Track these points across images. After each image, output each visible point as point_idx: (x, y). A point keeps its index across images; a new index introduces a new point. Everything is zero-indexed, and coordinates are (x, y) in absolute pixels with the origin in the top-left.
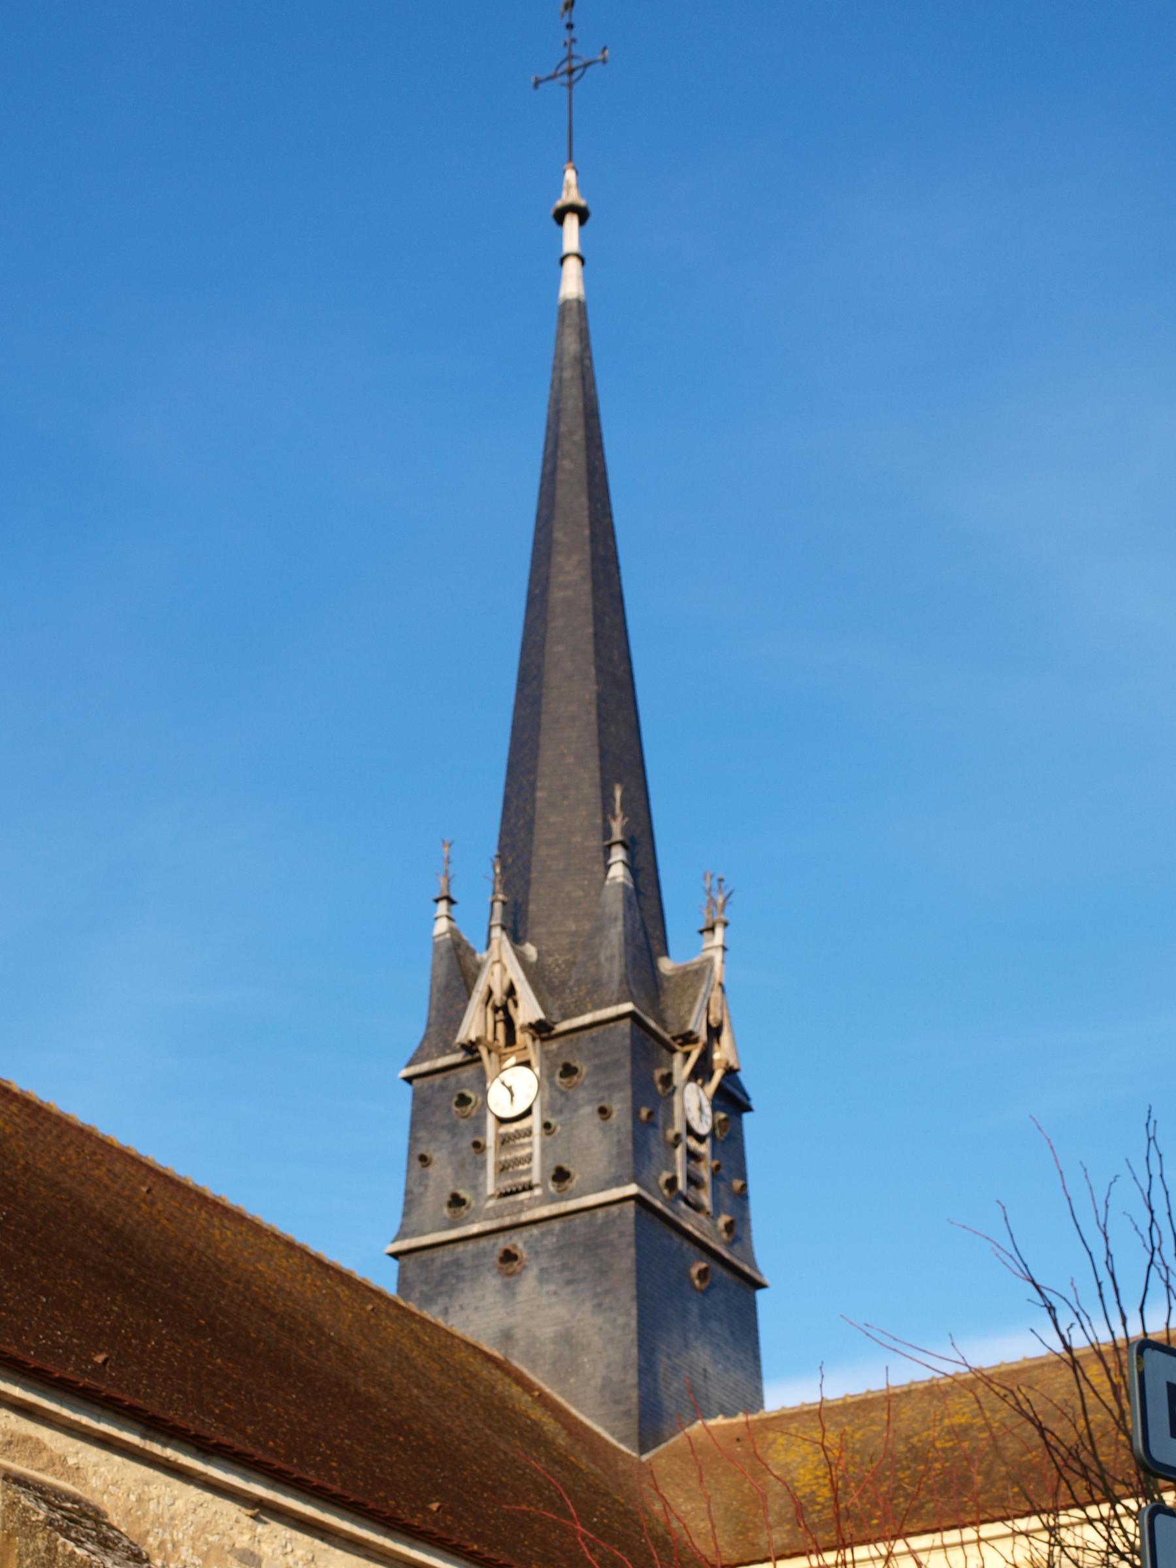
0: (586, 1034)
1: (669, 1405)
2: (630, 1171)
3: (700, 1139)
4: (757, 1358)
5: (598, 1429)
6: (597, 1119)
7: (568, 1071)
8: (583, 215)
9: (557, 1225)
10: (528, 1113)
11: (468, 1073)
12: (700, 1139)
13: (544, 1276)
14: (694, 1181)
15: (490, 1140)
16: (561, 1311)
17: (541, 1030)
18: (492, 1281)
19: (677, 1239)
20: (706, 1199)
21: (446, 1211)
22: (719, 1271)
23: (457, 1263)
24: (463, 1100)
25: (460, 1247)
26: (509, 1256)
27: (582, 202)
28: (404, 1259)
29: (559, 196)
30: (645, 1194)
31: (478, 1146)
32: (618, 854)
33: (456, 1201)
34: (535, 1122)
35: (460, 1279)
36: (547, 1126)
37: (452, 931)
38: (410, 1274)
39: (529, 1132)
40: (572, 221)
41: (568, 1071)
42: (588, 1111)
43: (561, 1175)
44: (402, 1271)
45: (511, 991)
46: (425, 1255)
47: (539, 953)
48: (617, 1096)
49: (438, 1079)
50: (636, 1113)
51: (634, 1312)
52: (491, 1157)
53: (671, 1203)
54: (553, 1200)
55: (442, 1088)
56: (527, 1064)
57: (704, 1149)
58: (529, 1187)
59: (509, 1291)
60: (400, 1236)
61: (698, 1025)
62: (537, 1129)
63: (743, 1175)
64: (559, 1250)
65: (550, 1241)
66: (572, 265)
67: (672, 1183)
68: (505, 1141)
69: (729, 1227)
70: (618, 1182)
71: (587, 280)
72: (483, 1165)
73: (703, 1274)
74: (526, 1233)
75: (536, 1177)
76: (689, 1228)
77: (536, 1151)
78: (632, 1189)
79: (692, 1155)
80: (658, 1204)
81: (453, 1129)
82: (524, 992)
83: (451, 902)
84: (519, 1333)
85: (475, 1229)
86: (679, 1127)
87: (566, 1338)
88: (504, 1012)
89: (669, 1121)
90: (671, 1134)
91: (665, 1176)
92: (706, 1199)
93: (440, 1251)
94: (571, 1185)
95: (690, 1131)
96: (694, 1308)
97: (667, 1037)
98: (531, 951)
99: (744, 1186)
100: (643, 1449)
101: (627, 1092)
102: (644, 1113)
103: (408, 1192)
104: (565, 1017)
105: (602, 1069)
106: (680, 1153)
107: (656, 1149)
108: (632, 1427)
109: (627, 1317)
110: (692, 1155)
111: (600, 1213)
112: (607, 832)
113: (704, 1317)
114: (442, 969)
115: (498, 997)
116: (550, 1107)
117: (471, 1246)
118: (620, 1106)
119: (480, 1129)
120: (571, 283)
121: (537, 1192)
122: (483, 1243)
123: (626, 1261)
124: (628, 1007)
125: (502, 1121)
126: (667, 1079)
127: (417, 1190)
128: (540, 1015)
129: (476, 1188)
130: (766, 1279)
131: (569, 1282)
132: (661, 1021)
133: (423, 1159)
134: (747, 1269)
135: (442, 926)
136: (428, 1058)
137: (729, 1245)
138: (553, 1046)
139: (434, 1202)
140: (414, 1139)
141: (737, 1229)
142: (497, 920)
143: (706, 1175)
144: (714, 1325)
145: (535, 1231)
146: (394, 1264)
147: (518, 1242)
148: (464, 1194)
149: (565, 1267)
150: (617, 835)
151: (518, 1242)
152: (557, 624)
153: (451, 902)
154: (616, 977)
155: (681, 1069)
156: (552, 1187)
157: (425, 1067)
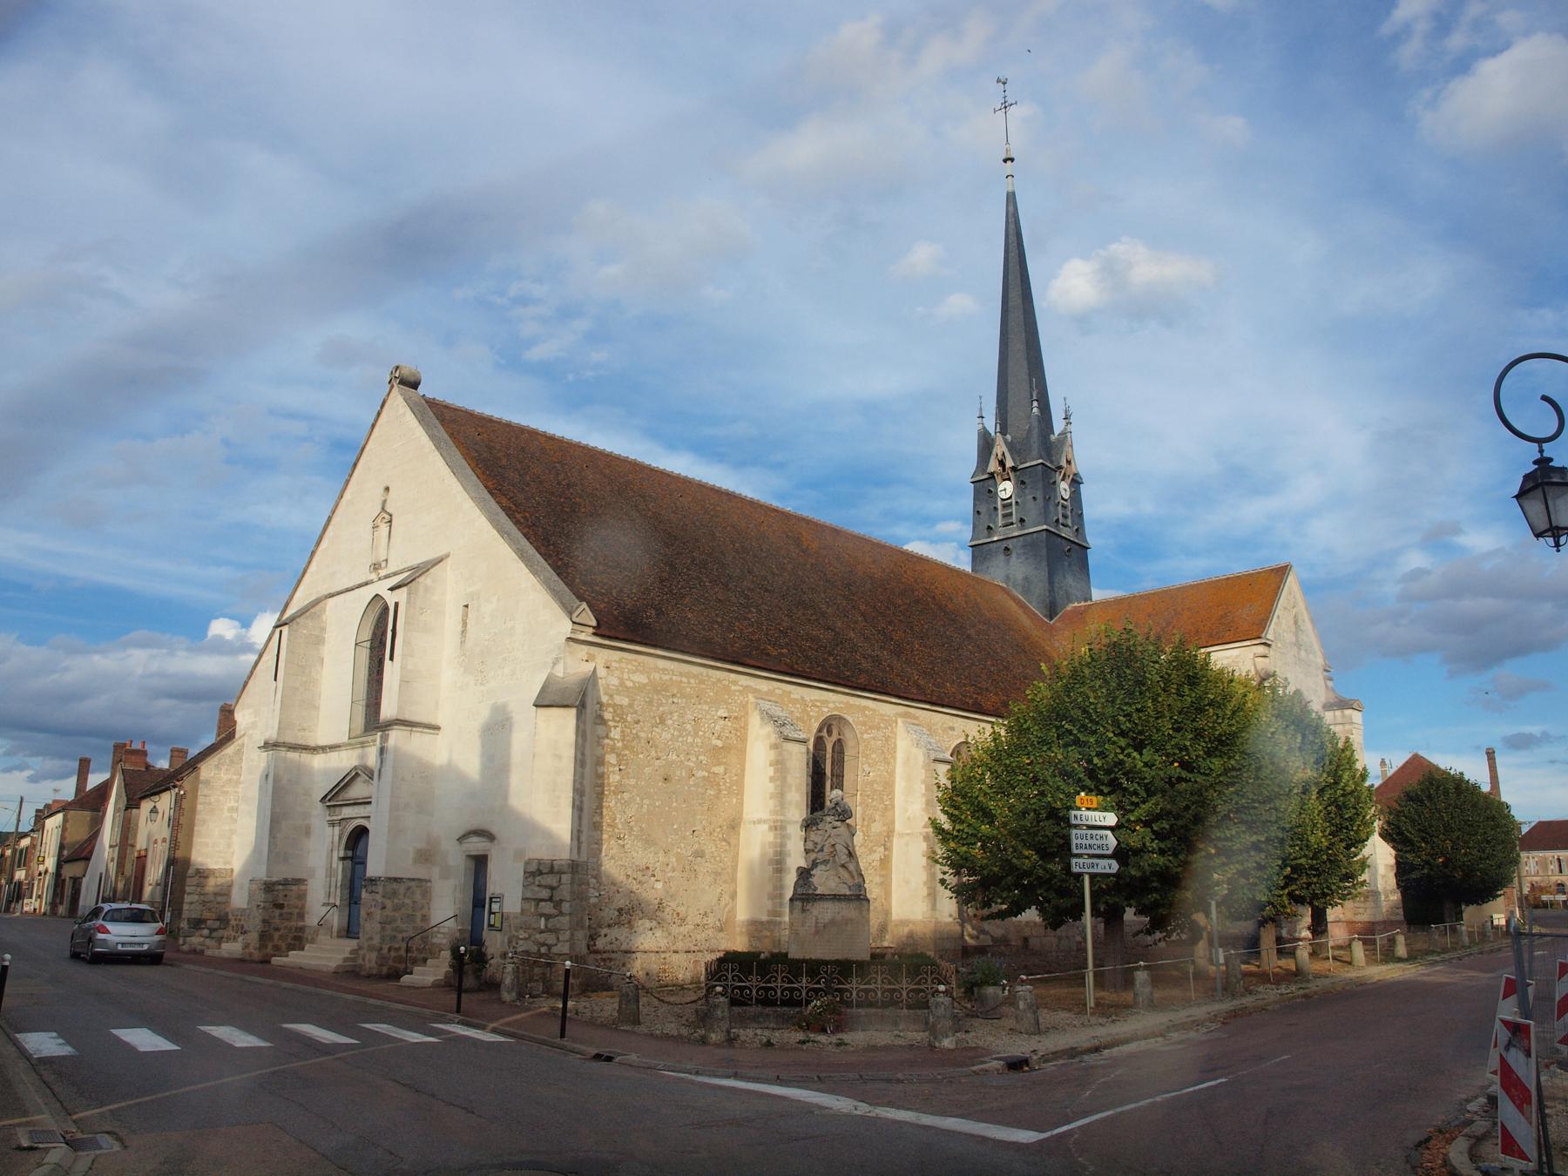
0: (1029, 469)
3: (1066, 500)
6: (1032, 500)
7: (1023, 483)
9: (1021, 539)
10: (1010, 497)
11: (991, 481)
12: (1066, 500)
14: (1065, 516)
15: (999, 506)
17: (1014, 469)
18: (1002, 557)
19: (1059, 539)
21: (986, 531)
23: (990, 550)
24: (990, 491)
25: (991, 545)
26: (1007, 549)
30: (1049, 528)
31: (996, 509)
32: (1035, 404)
33: (989, 528)
36: (1017, 502)
39: (1011, 504)
41: (1023, 483)
42: (1030, 497)
43: (1022, 521)
44: (973, 552)
47: (1012, 437)
48: (1038, 493)
51: (1047, 570)
52: (1000, 513)
53: (1056, 527)
56: (1009, 479)
58: (1012, 524)
59: (1008, 561)
61: (1064, 463)
64: (1024, 546)
67: (1057, 521)
68: (1004, 506)
69: (1077, 530)
72: (997, 515)
74: (1012, 540)
75: (1014, 519)
76: (1063, 535)
79: (1064, 507)
80: (1053, 530)
82: (1008, 455)
84: (1011, 577)
85: (995, 539)
87: (1026, 579)
88: (1002, 463)
89: (1055, 497)
91: (1055, 518)
92: (1069, 522)
93: (985, 546)
94: (1026, 524)
95: (1063, 499)
96: (1066, 563)
97: (1053, 467)
98: (1009, 437)
99: (1082, 513)
100: (1051, 619)
103: (974, 524)
104: (1022, 463)
109: (1044, 574)
111: (1035, 535)
112: (1032, 396)
113: (1070, 565)
114: (981, 443)
115: (1000, 457)
116: (1018, 496)
117: (994, 544)
118: (1039, 495)
119: (996, 502)
121: (1015, 526)
122: (999, 543)
123: (1044, 552)
124: (1040, 461)
125: (1003, 500)
127: (977, 523)
129: (995, 523)
130: (1091, 545)
131: (1027, 559)
132: (1051, 462)
133: (978, 512)
134: (1084, 544)
136: (978, 475)
138: (1018, 473)
139: (983, 528)
140: (975, 505)
141: (1079, 531)
142: (998, 430)
143: (1069, 513)
145: (1015, 540)
146: (971, 549)
147: (1010, 544)
148: (991, 525)
150: (1035, 398)
151: (1010, 544)
153: (983, 417)
157: (977, 479)
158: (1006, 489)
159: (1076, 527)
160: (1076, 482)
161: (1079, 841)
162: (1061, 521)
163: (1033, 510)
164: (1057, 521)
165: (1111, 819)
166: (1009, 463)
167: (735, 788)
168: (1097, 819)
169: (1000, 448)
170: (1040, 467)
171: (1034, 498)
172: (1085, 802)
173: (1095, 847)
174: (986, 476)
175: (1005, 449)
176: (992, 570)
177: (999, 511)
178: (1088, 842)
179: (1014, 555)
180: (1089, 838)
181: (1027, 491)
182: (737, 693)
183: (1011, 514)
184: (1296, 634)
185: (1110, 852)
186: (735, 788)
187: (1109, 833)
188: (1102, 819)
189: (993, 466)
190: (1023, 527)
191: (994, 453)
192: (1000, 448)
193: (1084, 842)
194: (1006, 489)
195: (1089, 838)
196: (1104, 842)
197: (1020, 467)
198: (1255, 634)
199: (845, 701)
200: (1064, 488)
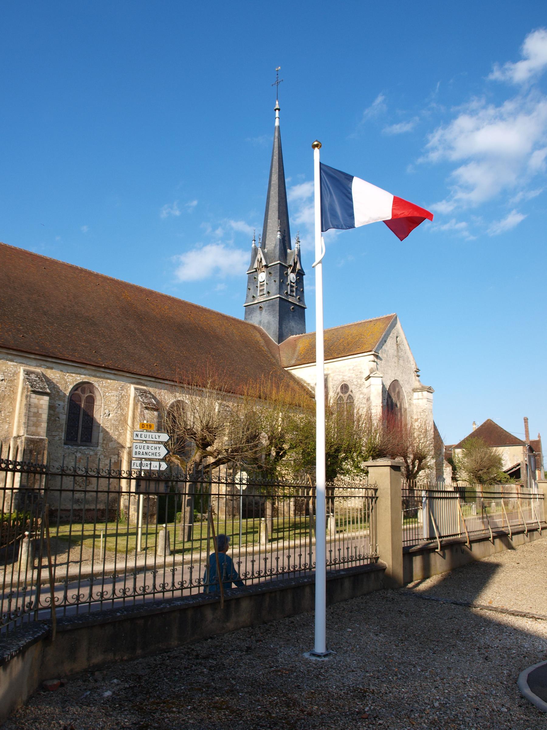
0: (273, 266)
1: (285, 334)
2: (278, 292)
3: (294, 283)
4: (305, 322)
5: (272, 339)
7: (270, 273)
8: (279, 110)
9: (268, 302)
10: (264, 281)
11: (256, 273)
12: (294, 283)
13: (265, 312)
14: (292, 291)
15: (259, 286)
16: (268, 317)
17: (266, 266)
18: (258, 311)
20: (294, 294)
22: (297, 307)
23: (253, 308)
24: (255, 278)
25: (254, 305)
26: (261, 307)
27: (278, 108)
28: (247, 307)
29: (275, 107)
30: (281, 296)
31: (257, 287)
33: (253, 297)
34: (265, 283)
35: (254, 311)
37: (255, 246)
38: (247, 310)
39: (264, 284)
40: (277, 111)
41: (270, 273)
42: (273, 280)
43: (268, 293)
45: (261, 259)
46: (249, 307)
49: (251, 274)
50: (280, 281)
52: (259, 289)
54: (267, 297)
55: (252, 276)
56: (264, 272)
57: (294, 285)
58: (264, 294)
59: (261, 314)
60: (245, 303)
62: (265, 284)
63: (303, 288)
64: (269, 306)
65: (267, 305)
66: (277, 120)
67: (287, 293)
68: (261, 286)
69: (299, 298)
70: (276, 294)
71: (280, 122)
73: (293, 308)
75: (265, 293)
76: (290, 300)
77: (265, 288)
78: (278, 296)
79: (292, 286)
80: (283, 297)
81: (253, 283)
83: (255, 240)
84: (262, 321)
85: (256, 302)
86: (289, 282)
89: (287, 281)
90: (287, 283)
91: (286, 291)
95: (291, 282)
96: (291, 315)
97: (287, 265)
100: (279, 343)
101: (278, 278)
102: (282, 280)
105: (275, 273)
106: (289, 287)
107: (284, 286)
108: (277, 340)
110: (292, 286)
113: (293, 316)
114: (253, 253)
115: (259, 260)
116: (268, 280)
117: (255, 305)
119: (257, 284)
120: (277, 123)
121: (265, 295)
122: (257, 304)
123: (277, 308)
124: (279, 262)
126: (287, 273)
128: (265, 264)
129: (256, 294)
130: (307, 307)
131: (269, 312)
135: (253, 245)
137: (299, 302)
138: (268, 269)
139: (251, 297)
140: (248, 285)
141: (301, 299)
143: (294, 289)
144: (296, 317)
148: (255, 296)
149: (269, 309)
152: (272, 188)
154: (278, 256)
155: (289, 270)
156: (267, 295)
158: (262, 276)
159: (298, 297)
160: (300, 274)
161: (138, 450)
162: (289, 293)
163: (274, 287)
164: (287, 293)
165: (165, 437)
166: (264, 263)
167: (8, 419)
168: (154, 437)
169: (260, 255)
170: (279, 265)
171: (275, 281)
172: (146, 426)
173: (150, 454)
174: (255, 270)
175: (262, 256)
176: (253, 318)
177: (259, 288)
178: (144, 451)
179: (264, 310)
180: (146, 448)
181: (272, 278)
182: (12, 366)
183: (263, 289)
184: (398, 351)
185: (161, 457)
186: (8, 419)
187: (162, 446)
188: (157, 437)
189: (256, 266)
190: (269, 296)
191: (257, 258)
192: (260, 255)
193: (142, 451)
194: (262, 276)
195: (146, 448)
196: (158, 451)
197: (269, 265)
198: (369, 349)
199: (93, 374)
200: (292, 277)
